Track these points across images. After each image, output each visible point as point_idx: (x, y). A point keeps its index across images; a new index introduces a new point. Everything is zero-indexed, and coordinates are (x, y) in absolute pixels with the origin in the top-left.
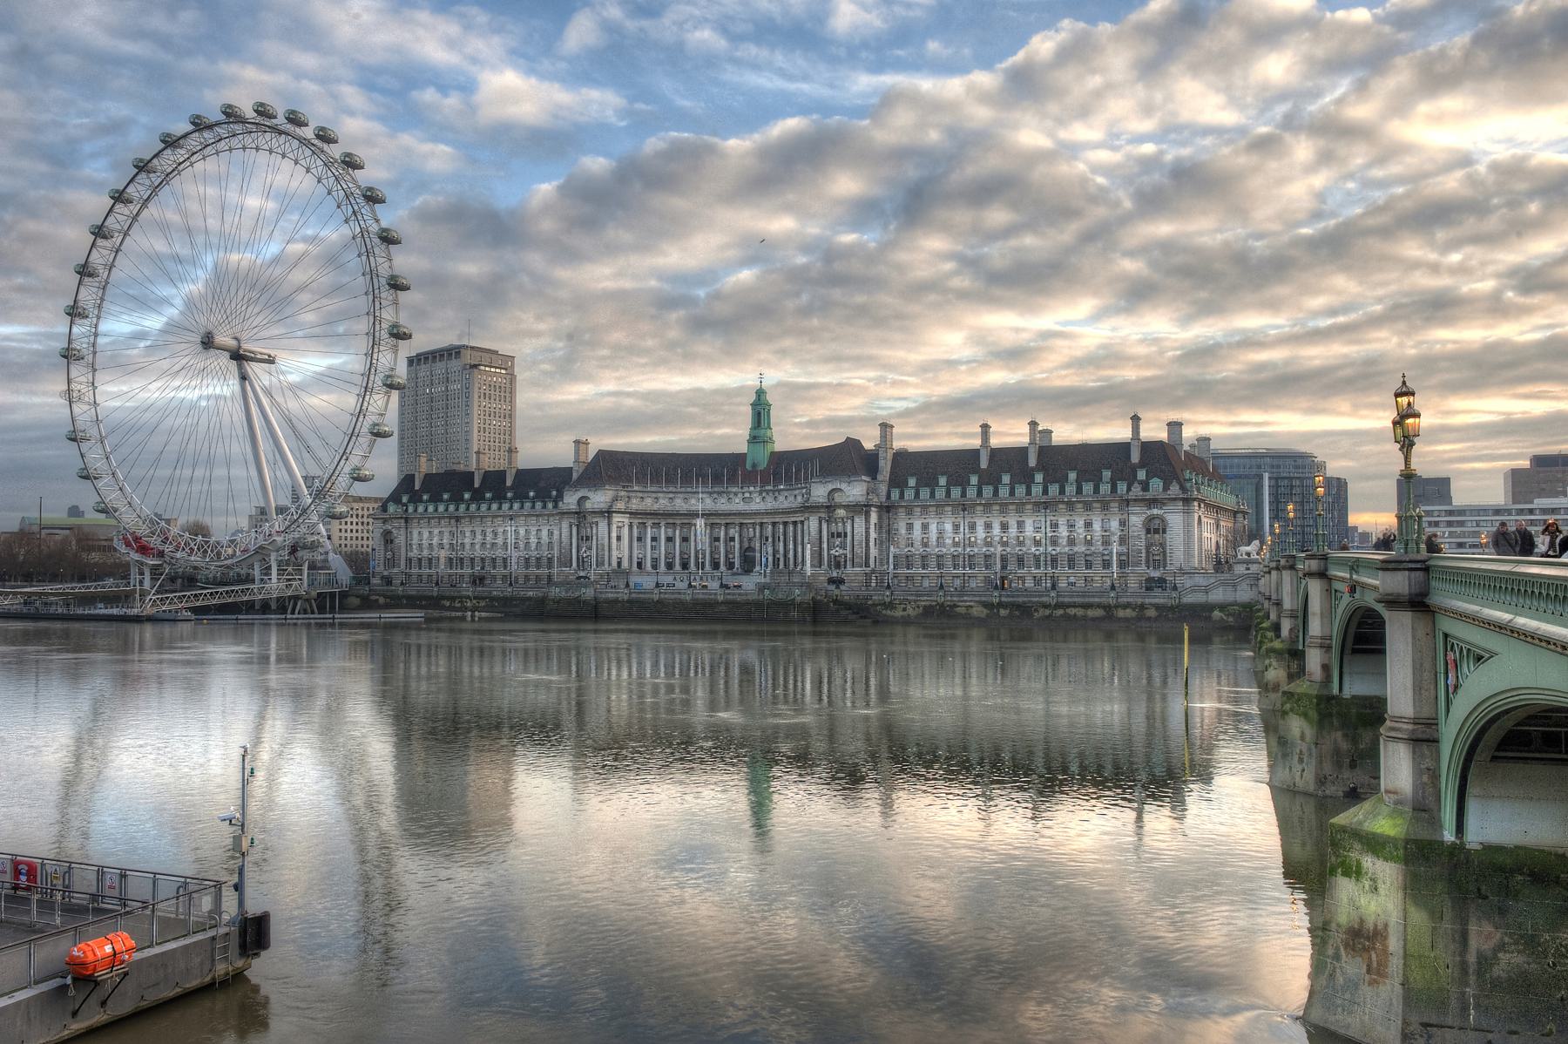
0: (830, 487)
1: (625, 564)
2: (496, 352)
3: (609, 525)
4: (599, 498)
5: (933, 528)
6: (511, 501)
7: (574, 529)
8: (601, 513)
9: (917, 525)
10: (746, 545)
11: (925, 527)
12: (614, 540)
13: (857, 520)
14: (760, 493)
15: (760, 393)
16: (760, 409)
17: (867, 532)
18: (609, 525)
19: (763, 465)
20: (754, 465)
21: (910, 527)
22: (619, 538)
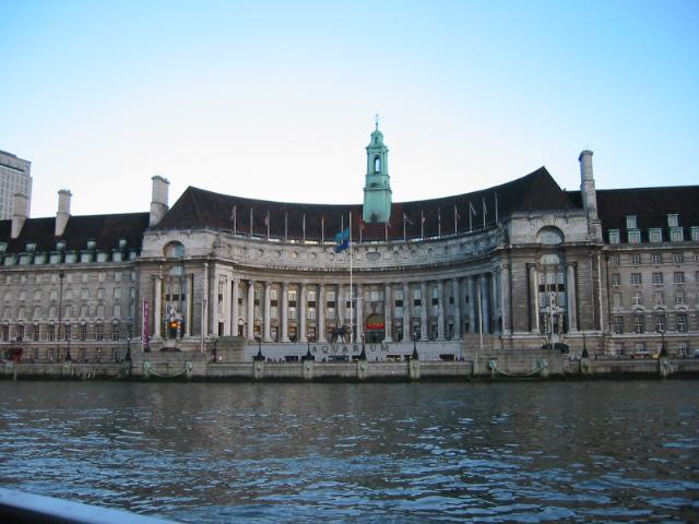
0: (540, 224)
1: (227, 332)
2: (14, 157)
3: (211, 277)
4: (196, 243)
5: (669, 277)
6: (63, 254)
7: (159, 285)
8: (199, 262)
9: (647, 274)
10: (370, 311)
11: (658, 277)
12: (216, 299)
13: (582, 266)
14: (390, 247)
15: (376, 136)
16: (377, 151)
17: (596, 285)
18: (209, 278)
19: (386, 217)
20: (374, 217)
21: (637, 278)
22: (220, 297)
